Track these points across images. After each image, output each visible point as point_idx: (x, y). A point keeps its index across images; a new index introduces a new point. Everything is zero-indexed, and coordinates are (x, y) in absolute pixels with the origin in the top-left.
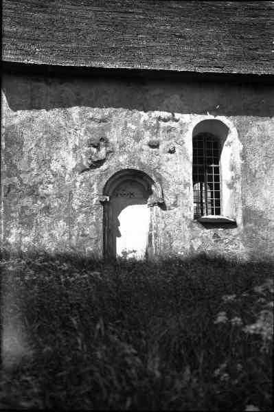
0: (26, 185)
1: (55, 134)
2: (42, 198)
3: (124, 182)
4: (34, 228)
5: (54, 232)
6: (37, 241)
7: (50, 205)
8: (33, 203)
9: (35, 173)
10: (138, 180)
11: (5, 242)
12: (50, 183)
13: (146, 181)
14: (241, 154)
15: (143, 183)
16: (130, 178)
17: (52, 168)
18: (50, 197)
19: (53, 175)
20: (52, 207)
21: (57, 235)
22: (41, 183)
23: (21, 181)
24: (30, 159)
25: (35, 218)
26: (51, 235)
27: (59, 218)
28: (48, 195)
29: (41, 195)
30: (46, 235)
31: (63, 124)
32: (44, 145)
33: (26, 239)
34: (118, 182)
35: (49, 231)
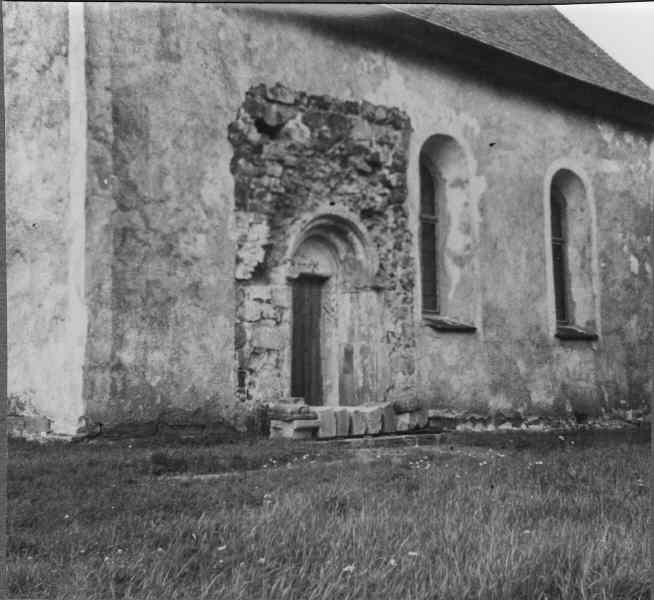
0: (156, 231)
1: (207, 122)
2: (187, 264)
4: (171, 332)
5: (206, 341)
6: (178, 360)
7: (200, 282)
8: (169, 274)
9: (172, 204)
11: (116, 361)
12: (200, 231)
14: (479, 205)
16: (324, 234)
17: (205, 198)
18: (201, 263)
19: (206, 212)
20: (205, 284)
21: (213, 348)
22: (184, 230)
23: (146, 220)
24: (163, 173)
25: (172, 309)
26: (203, 348)
27: (214, 311)
28: (196, 259)
29: (186, 257)
30: (193, 348)
31: (222, 102)
32: (190, 143)
33: (156, 357)
35: (199, 338)
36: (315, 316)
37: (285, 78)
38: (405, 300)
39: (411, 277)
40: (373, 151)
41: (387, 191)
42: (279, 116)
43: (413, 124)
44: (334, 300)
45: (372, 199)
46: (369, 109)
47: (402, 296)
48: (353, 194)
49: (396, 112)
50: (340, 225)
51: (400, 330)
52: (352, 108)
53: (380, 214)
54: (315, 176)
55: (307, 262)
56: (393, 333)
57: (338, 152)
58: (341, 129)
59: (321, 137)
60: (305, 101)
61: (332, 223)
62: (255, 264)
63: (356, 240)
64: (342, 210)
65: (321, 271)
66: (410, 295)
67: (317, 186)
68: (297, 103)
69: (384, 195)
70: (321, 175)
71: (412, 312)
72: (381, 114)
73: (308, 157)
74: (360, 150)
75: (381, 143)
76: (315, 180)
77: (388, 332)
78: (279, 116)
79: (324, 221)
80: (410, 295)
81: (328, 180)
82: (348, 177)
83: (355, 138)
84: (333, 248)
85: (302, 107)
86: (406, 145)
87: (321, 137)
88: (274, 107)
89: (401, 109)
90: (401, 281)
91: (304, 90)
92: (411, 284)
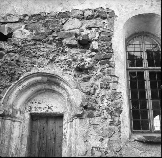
3: (39, 92)
10: (55, 88)
13: (64, 89)
15: (60, 90)
16: (47, 86)
34: (30, 92)
36: (57, 141)
37: (13, 10)
38: (111, 123)
39: (118, 106)
40: (84, 34)
41: (94, 53)
42: (9, 29)
43: (116, 13)
44: (65, 128)
45: (82, 60)
46: (77, 13)
47: (109, 121)
48: (65, 60)
49: (101, 10)
50: (51, 79)
51: (106, 145)
52: (65, 15)
53: (92, 68)
54: (37, 55)
55: (43, 106)
56: (98, 149)
57: (51, 38)
58: (53, 26)
59: (37, 33)
60: (27, 18)
61: (45, 79)
63: (66, 87)
64: (56, 70)
65: (57, 109)
66: (117, 119)
67: (39, 61)
68: (21, 21)
69: (92, 56)
70: (41, 53)
71: (120, 131)
72: (90, 13)
73: (32, 45)
74: (69, 35)
75: (90, 28)
76: (38, 57)
77: (93, 147)
78: (9, 29)
79: (39, 78)
80: (117, 119)
81: (48, 55)
82: (62, 51)
83: (66, 30)
84: (59, 94)
85: (25, 21)
86: (112, 25)
87: (37, 33)
88: (6, 26)
89: (105, 7)
90: (107, 110)
91: (26, 13)
92: (119, 111)
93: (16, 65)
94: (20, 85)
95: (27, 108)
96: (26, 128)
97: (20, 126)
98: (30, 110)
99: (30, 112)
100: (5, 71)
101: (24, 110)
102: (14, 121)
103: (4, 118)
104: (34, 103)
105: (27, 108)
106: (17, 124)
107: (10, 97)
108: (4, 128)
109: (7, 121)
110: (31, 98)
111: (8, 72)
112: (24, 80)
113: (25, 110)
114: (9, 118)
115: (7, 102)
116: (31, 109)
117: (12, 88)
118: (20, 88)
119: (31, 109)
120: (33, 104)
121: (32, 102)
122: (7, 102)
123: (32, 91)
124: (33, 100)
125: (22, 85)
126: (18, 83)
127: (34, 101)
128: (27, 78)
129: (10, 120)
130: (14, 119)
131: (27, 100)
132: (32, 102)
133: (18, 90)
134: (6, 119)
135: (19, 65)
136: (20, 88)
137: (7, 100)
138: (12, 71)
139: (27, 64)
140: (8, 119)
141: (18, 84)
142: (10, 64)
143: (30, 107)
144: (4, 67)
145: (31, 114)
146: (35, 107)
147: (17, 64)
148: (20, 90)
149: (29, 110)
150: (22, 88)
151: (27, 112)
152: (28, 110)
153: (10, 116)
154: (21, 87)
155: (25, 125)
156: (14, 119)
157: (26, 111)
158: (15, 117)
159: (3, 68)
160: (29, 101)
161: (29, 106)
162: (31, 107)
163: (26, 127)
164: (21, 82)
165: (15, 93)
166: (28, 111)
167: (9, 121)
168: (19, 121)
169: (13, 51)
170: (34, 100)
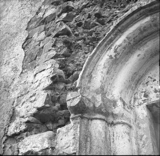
62: (34, 111)
93: (97, 23)
94: (110, 48)
95: (138, 96)
96: (147, 138)
97: (129, 134)
98: (145, 100)
99: (146, 104)
100: (80, 40)
101: (132, 102)
102: (112, 124)
103: (86, 115)
104: (151, 83)
105: (138, 96)
106: (120, 129)
107: (93, 76)
108: (89, 139)
109: (95, 121)
110: (141, 73)
111: (84, 39)
112: (116, 35)
113: (134, 101)
114: (98, 116)
115: (89, 85)
116: (146, 96)
117: (95, 56)
118: (111, 52)
119: (146, 96)
120: (149, 86)
121: (147, 83)
122: (89, 85)
123: (138, 56)
124: (146, 79)
125: (113, 47)
126: (105, 43)
127: (150, 79)
128: (119, 28)
129: (100, 119)
130: (111, 119)
131: (132, 79)
132: (147, 83)
133: (108, 57)
134: (92, 119)
135: (103, 23)
136: (111, 52)
137: (89, 82)
138: (94, 35)
139: (116, 15)
140: (96, 119)
141: (106, 46)
142: (87, 26)
143: (144, 93)
144: (77, 33)
145: (150, 108)
146: (155, 89)
147: (98, 21)
148: (111, 57)
149: (144, 98)
150: (115, 51)
151: (140, 104)
152: (140, 101)
153: (98, 111)
154: (112, 51)
155: (141, 132)
156: (111, 119)
157: (136, 104)
158: (114, 116)
159: (76, 35)
160: (140, 82)
161: (142, 92)
162: (145, 92)
163: (145, 136)
164: (111, 41)
165: (103, 64)
166: (142, 102)
167: (98, 122)
168: (124, 124)
169: (89, 5)
170: (149, 77)
